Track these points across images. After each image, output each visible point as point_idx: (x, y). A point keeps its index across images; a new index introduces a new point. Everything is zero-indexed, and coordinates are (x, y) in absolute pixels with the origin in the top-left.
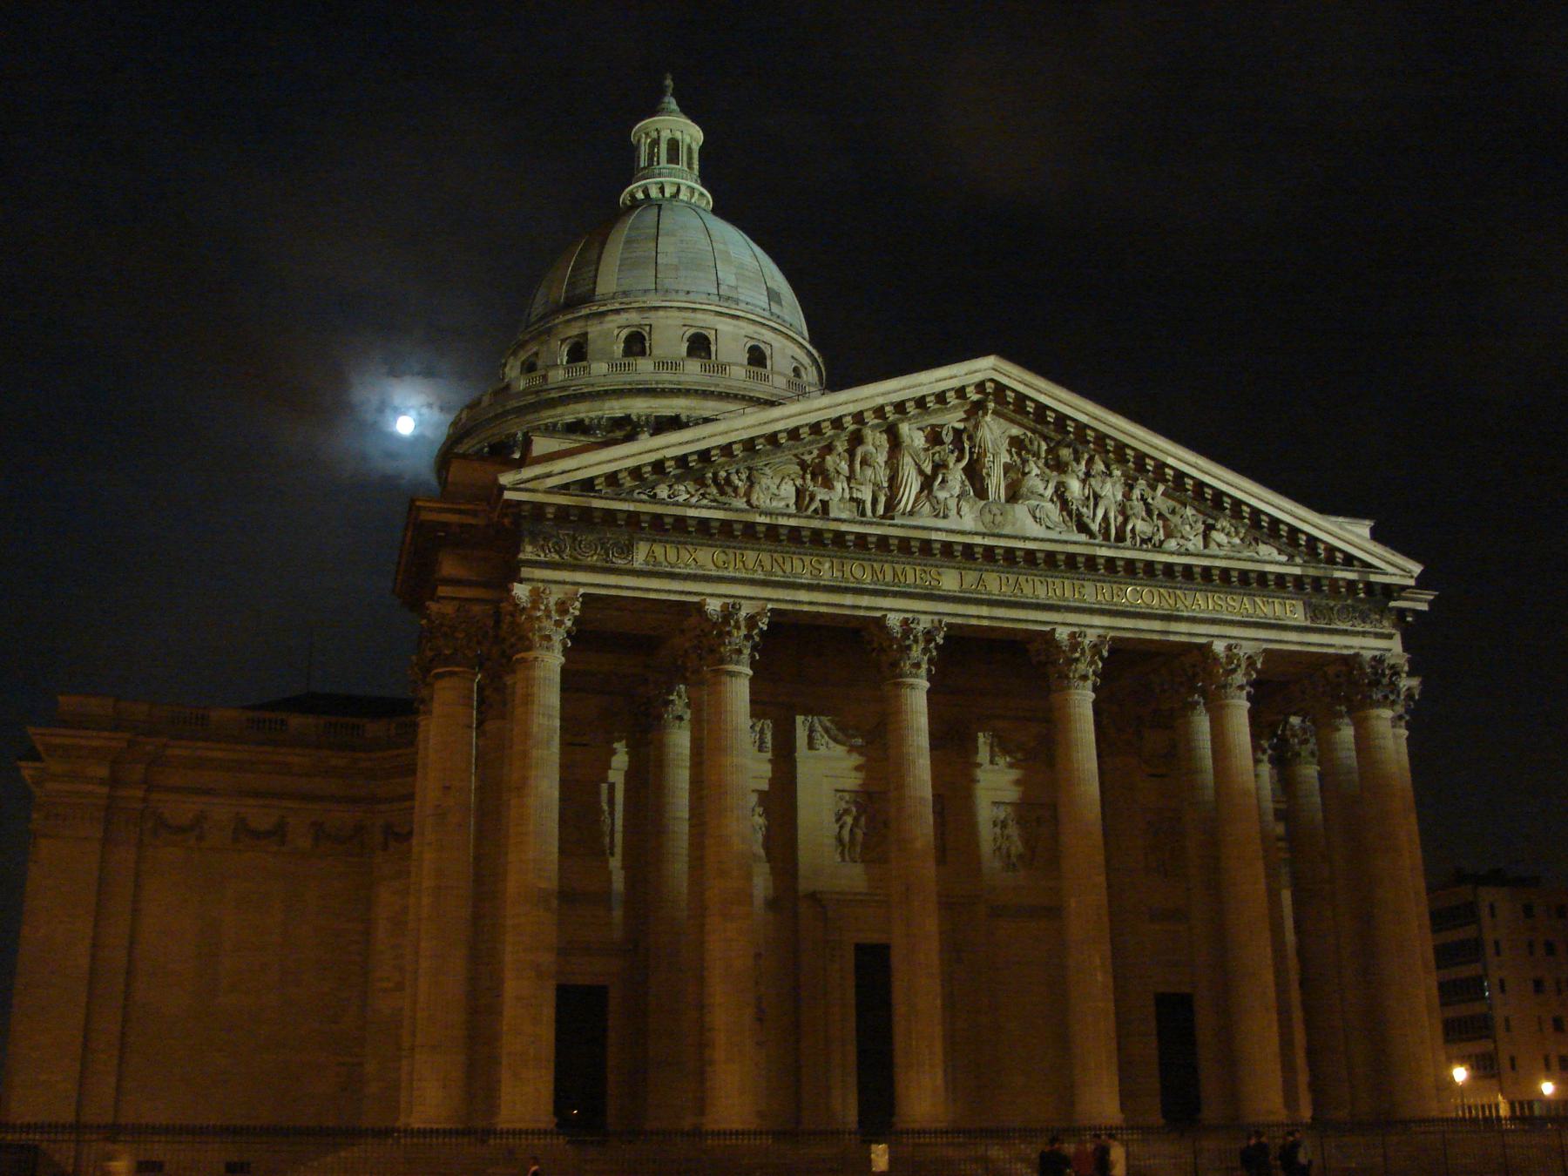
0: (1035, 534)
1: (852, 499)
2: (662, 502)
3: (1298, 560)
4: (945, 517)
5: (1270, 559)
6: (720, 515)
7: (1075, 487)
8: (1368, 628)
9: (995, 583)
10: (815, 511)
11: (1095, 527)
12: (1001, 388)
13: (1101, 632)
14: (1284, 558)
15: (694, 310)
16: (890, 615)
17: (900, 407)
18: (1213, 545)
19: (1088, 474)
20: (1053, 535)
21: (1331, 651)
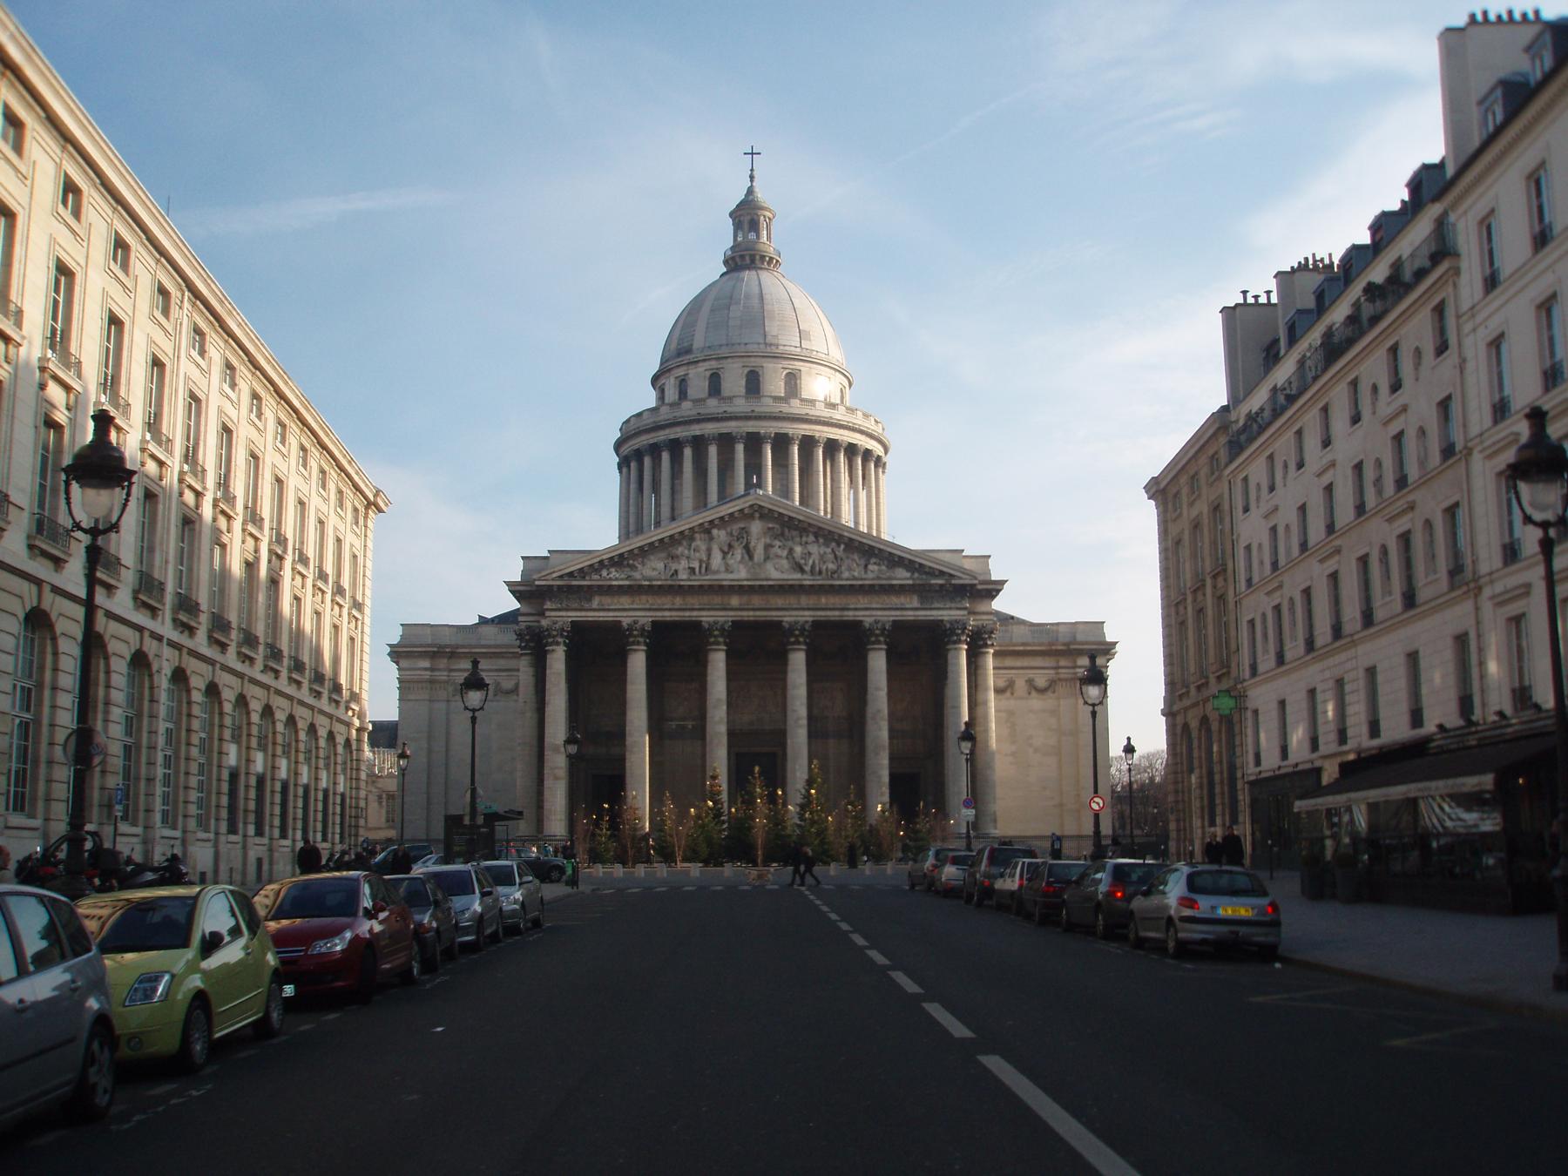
7: (798, 549)
9: (757, 601)
11: (807, 568)
14: (908, 575)
20: (785, 576)
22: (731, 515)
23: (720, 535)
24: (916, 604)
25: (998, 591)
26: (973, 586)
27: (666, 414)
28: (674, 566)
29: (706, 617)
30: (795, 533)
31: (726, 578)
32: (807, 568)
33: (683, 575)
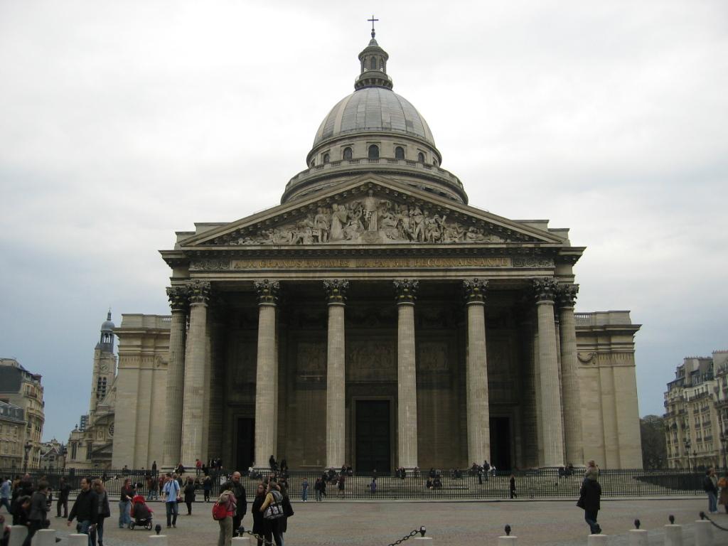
0: (387, 243)
1: (313, 236)
2: (241, 245)
3: (509, 241)
4: (349, 239)
5: (496, 242)
6: (259, 248)
7: (406, 220)
8: (541, 266)
9: (371, 264)
10: (298, 242)
11: (415, 236)
12: (375, 185)
13: (415, 278)
14: (502, 241)
15: (371, 136)
16: (327, 279)
17: (332, 198)
18: (468, 239)
19: (413, 215)
21: (524, 278)
22: (349, 192)
23: (341, 210)
24: (509, 266)
25: (579, 256)
26: (559, 249)
27: (314, 173)
28: (301, 234)
29: (328, 277)
30: (403, 207)
31: (344, 244)
32: (415, 236)
33: (307, 241)
